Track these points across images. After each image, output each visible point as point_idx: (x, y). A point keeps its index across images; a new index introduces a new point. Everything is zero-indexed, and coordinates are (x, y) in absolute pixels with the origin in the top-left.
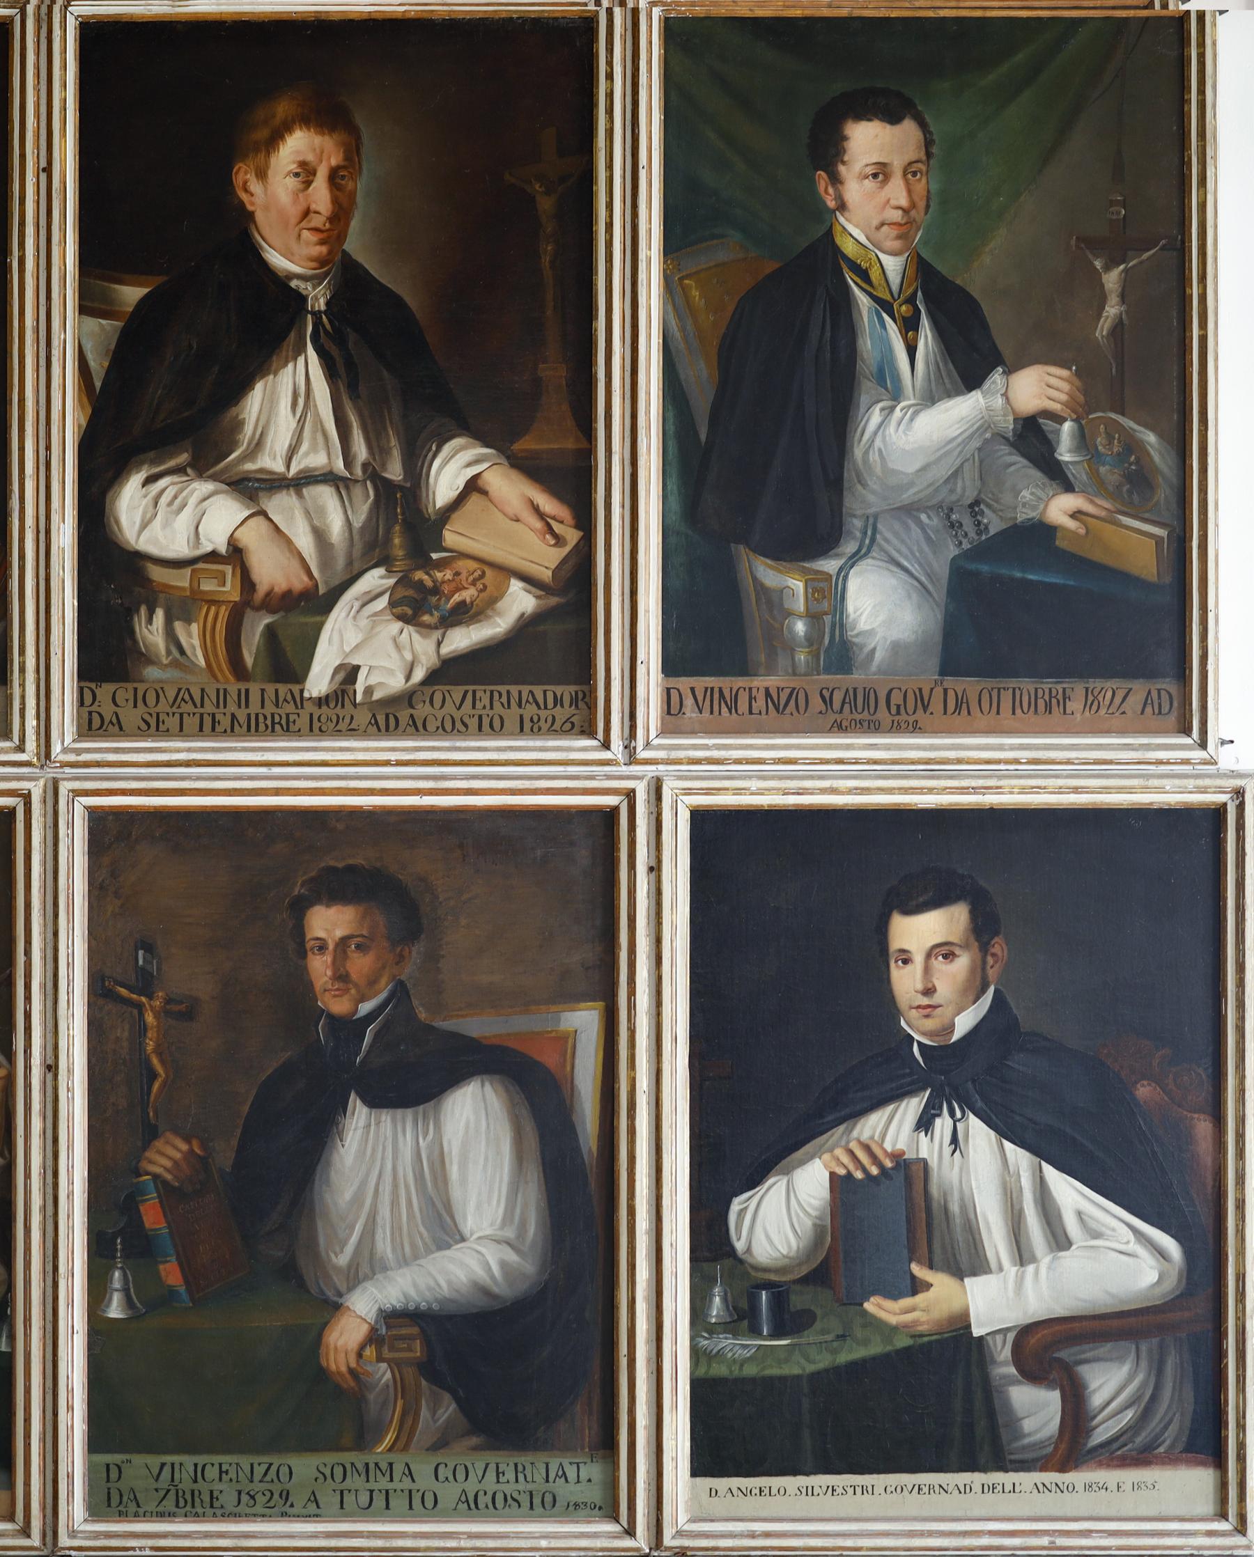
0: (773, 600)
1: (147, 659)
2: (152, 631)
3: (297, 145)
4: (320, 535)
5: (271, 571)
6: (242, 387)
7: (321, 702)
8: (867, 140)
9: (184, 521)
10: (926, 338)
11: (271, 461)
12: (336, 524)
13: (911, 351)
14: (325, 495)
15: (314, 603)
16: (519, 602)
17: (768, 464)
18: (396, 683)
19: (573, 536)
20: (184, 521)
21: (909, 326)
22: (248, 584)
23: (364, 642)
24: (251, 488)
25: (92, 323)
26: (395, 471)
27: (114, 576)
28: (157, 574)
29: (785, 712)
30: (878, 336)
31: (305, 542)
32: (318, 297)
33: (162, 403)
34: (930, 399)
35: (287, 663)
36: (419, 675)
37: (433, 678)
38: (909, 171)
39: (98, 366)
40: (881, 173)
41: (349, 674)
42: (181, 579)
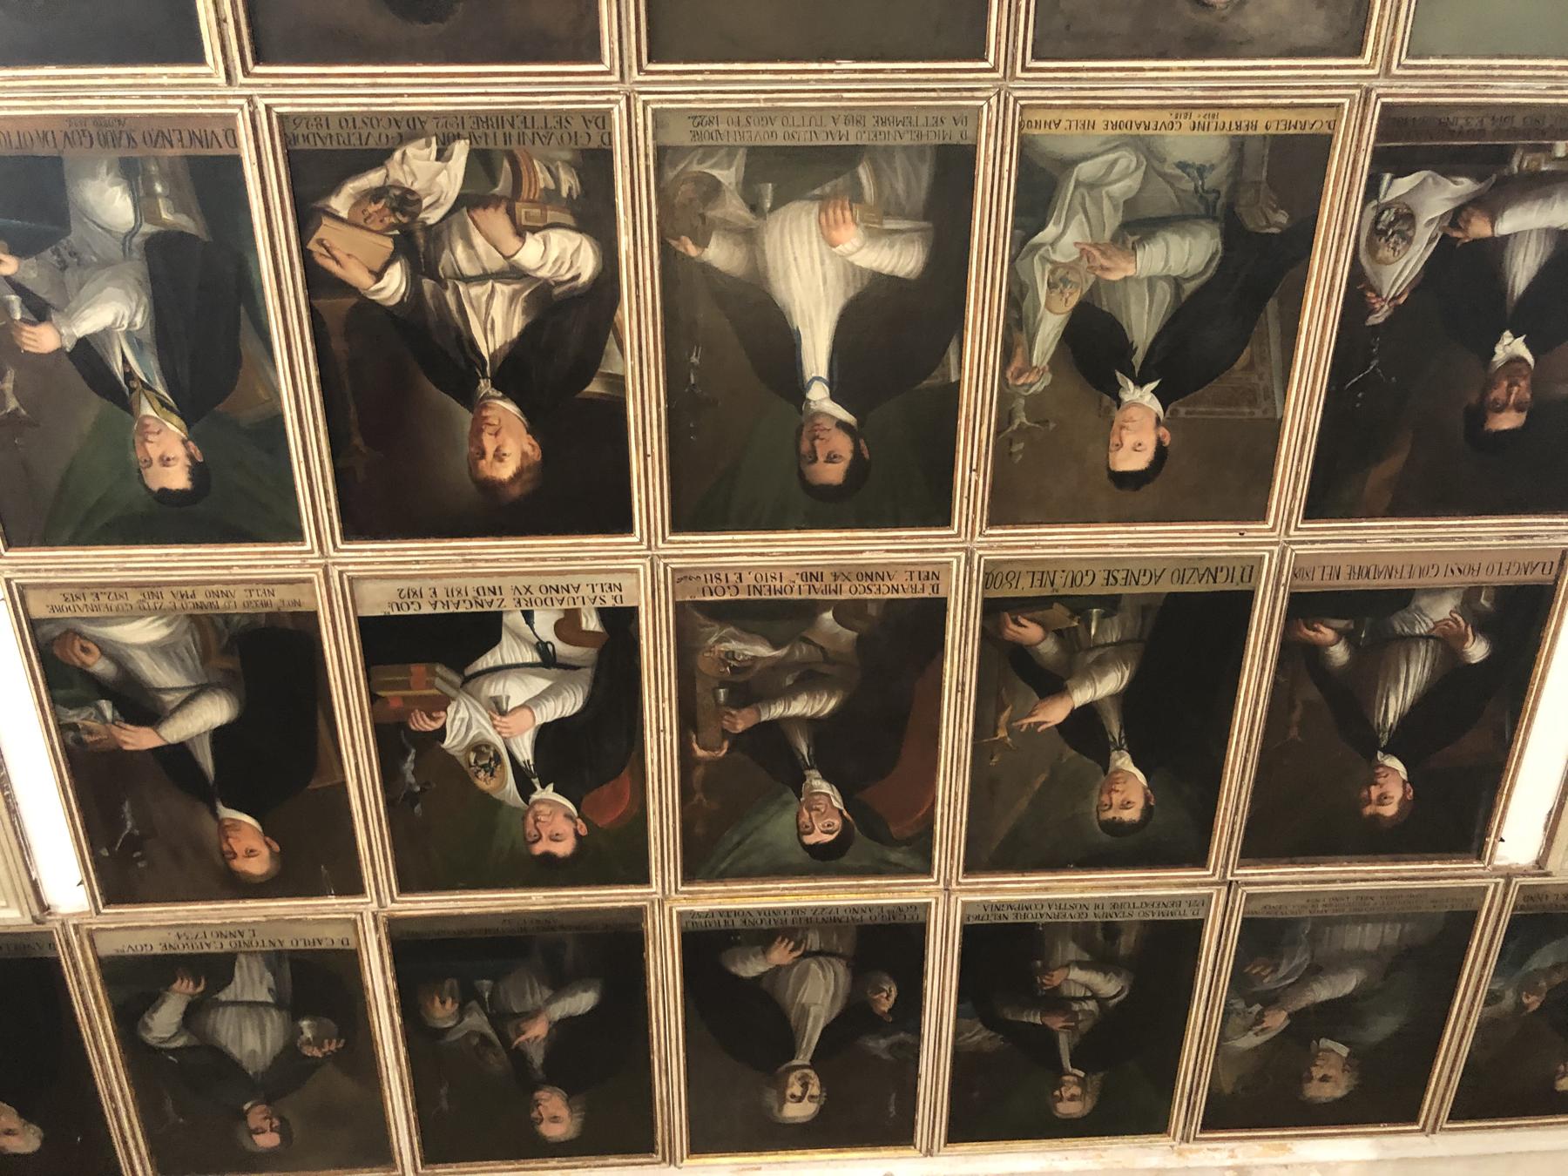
0: (179, 207)
1: (570, 164)
2: (568, 182)
3: (506, 471)
4: (469, 245)
5: (497, 221)
6: (524, 334)
7: (458, 137)
8: (177, 478)
9: (554, 253)
10: (118, 368)
11: (504, 291)
12: (460, 251)
13: (125, 360)
14: (468, 269)
15: (468, 201)
16: (340, 203)
18: (411, 150)
19: (312, 245)
20: (554, 253)
21: (129, 375)
22: (511, 213)
23: (434, 176)
24: (513, 273)
25: (617, 370)
26: (428, 284)
27: (593, 215)
28: (568, 219)
29: (159, 130)
30: (145, 368)
31: (478, 240)
32: (485, 386)
33: (569, 325)
34: (107, 332)
35: (481, 163)
36: (397, 155)
37: (389, 153)
38: (149, 463)
39: (611, 345)
40: (165, 461)
41: (442, 155)
42: (552, 216)
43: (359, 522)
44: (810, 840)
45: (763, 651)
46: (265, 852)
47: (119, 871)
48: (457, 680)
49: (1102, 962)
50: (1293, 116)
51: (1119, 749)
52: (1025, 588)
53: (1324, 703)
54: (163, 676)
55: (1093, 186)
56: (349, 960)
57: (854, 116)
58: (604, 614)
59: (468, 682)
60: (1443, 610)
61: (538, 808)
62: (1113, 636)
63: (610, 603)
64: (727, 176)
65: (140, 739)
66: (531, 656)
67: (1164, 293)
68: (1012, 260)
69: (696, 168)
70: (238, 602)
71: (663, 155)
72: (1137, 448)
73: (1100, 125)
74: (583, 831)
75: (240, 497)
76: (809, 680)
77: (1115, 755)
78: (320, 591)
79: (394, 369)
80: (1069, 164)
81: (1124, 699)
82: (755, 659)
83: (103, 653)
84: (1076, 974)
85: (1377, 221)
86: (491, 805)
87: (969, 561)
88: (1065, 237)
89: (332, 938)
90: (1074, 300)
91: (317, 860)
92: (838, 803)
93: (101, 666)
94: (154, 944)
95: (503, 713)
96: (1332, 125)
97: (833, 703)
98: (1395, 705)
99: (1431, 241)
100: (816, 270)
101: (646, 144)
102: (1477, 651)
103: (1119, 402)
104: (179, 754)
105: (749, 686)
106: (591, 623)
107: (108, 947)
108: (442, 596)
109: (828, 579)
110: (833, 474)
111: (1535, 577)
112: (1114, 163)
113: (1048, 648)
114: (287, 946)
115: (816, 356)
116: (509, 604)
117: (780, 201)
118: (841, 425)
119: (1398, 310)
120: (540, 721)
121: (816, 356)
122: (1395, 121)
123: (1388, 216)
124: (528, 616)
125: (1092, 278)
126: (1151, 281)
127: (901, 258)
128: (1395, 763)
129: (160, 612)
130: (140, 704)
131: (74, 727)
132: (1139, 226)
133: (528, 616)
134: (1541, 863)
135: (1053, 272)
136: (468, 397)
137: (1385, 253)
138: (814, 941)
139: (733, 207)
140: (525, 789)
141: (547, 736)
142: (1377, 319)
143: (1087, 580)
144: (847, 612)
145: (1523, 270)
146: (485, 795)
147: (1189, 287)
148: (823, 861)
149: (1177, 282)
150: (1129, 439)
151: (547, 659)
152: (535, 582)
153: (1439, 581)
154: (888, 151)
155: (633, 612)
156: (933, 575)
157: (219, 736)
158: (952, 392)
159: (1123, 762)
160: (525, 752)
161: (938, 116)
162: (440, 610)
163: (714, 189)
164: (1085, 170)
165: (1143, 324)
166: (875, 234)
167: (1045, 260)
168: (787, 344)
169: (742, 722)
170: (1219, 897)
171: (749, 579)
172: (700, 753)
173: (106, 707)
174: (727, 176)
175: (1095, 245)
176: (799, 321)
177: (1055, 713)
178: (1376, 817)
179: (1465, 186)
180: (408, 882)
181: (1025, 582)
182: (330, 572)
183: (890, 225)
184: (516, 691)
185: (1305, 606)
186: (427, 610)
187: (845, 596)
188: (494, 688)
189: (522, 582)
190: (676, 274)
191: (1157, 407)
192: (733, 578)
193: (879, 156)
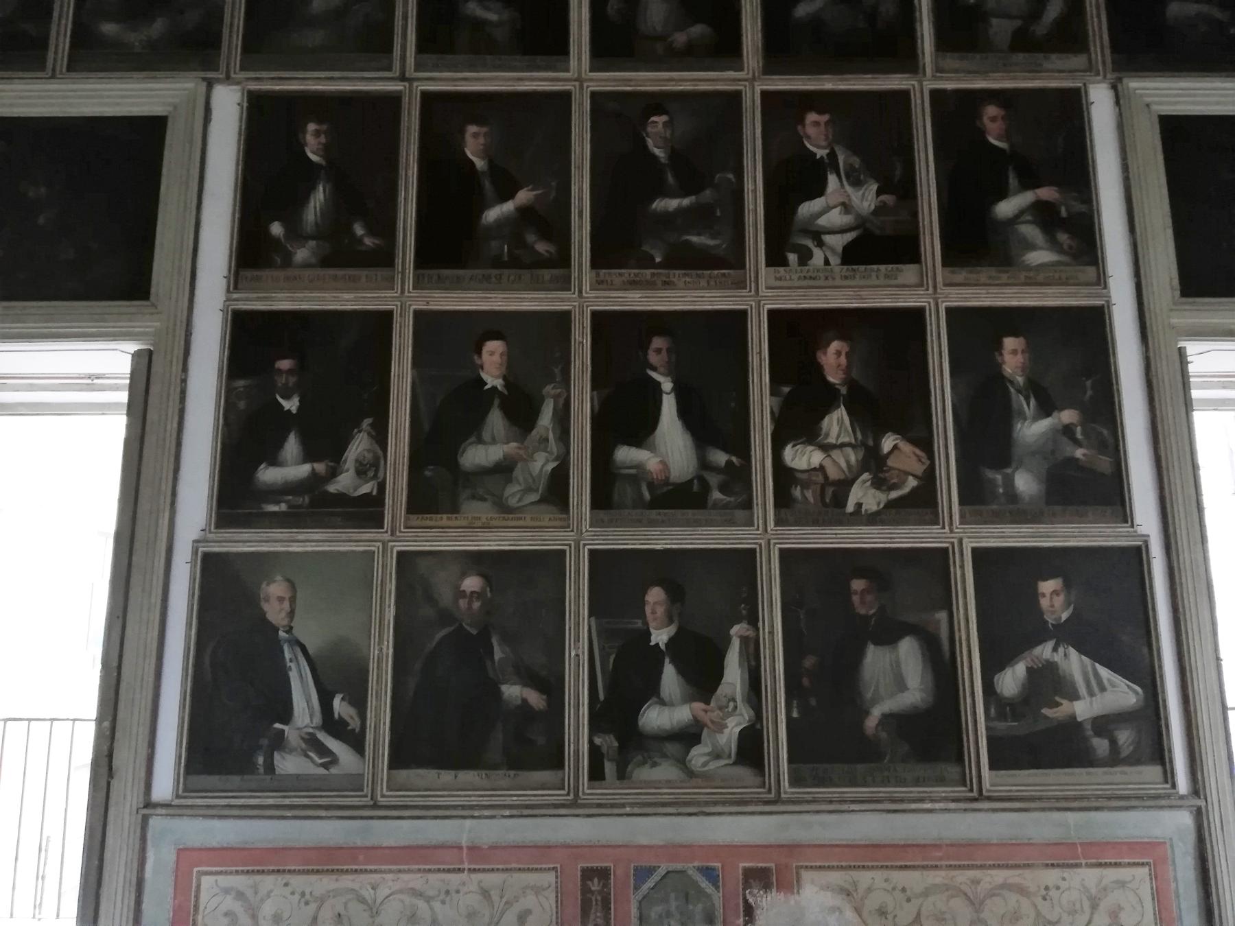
0: (992, 482)
1: (794, 500)
2: (797, 492)
3: (835, 345)
4: (848, 462)
5: (833, 474)
6: (823, 418)
7: (851, 514)
8: (1010, 343)
9: (805, 458)
10: (1033, 402)
11: (832, 440)
12: (853, 458)
13: (1028, 405)
14: (849, 450)
15: (845, 485)
16: (912, 483)
17: (986, 439)
18: (874, 508)
19: (928, 462)
20: (805, 458)
21: (1027, 399)
22: (826, 477)
23: (864, 495)
24: (826, 448)
25: (774, 399)
26: (871, 443)
27: (784, 477)
28: (799, 475)
29: (997, 518)
30: (1019, 400)
31: (844, 465)
32: (844, 390)
33: (797, 422)
34: (1036, 419)
35: (840, 500)
36: (882, 506)
37: (886, 506)
38: (1023, 352)
39: (776, 410)
40: (1014, 352)
41: (859, 505)
42: (804, 476)
43: (916, 317)
44: (664, 118)
45: (694, 239)
46: (986, 120)
47: (1071, 108)
48: (868, 225)
49: (479, 25)
50: (429, 523)
51: (483, 173)
52: (547, 274)
53: (363, 195)
54: (1030, 231)
55: (529, 490)
56: (944, 43)
57: (652, 523)
58: (784, 263)
59: (861, 224)
60: (301, 254)
61: (824, 143)
62: (494, 244)
63: (781, 269)
64: (716, 495)
65: (1047, 193)
66: (827, 238)
67: (486, 435)
68: (568, 452)
69: (732, 499)
70: (984, 274)
71: (748, 505)
72: (492, 354)
73: (528, 517)
74: (799, 128)
75: (977, 331)
76: (667, 218)
77: (486, 168)
78: (939, 279)
79: (890, 402)
80: (541, 501)
81: (484, 206)
82: (699, 234)
83: (1061, 245)
84: (493, 17)
85: (377, 472)
86: (854, 148)
87: (580, 292)
88: (542, 464)
89: (951, 61)
90: (534, 432)
91: (956, 112)
92: (650, 142)
93: (1063, 237)
94: (1056, 61)
95: (843, 204)
96: (407, 519)
97: (654, 206)
98: (319, 196)
99: (346, 461)
100: (671, 448)
101: (758, 511)
102: (276, 229)
103: (505, 378)
104: (1029, 183)
105: (700, 217)
106: (792, 257)
107: (1078, 61)
108: (874, 274)
109: (659, 283)
110: (658, 342)
111: (249, 273)
112: (520, 500)
113: (531, 238)
114: (978, 56)
115: (669, 405)
116: (837, 269)
117: (690, 482)
118: (654, 369)
119: (357, 424)
120: (823, 199)
121: (669, 405)
122: (376, 521)
123: (371, 474)
124: (827, 262)
125: (526, 443)
126: (494, 441)
127: (626, 454)
128: (314, 158)
129: (1028, 268)
130: (1044, 215)
131: (1083, 202)
132: (504, 469)
133: (827, 262)
134: (210, 84)
135: (546, 447)
136: (851, 383)
137: (369, 456)
138: (660, 48)
139: (714, 480)
140: (832, 155)
141: (818, 190)
142: (367, 422)
143: (512, 278)
144: (647, 262)
145: (292, 446)
146: (855, 153)
147: (473, 439)
148: (656, 103)
149: (480, 441)
150: (496, 358)
151: (817, 236)
152: (821, 283)
153: (308, 273)
154: (634, 507)
155: (769, 263)
156: (599, 284)
157: (1003, 194)
158: (596, 384)
159: (480, 164)
160: (832, 180)
161: (611, 523)
162: (875, 267)
163: (723, 488)
164: (534, 497)
165: (496, 420)
166: (639, 466)
167: (551, 453)
168: (684, 413)
169: (708, 195)
170: (410, 72)
171: (703, 283)
172: (731, 176)
173: (1064, 213)
174: (716, 495)
175: (525, 460)
176: (678, 424)
177: (524, 196)
178: (319, 121)
179: (332, 488)
180: (903, 97)
181: (547, 277)
182: (932, 291)
183: (633, 471)
184: (835, 218)
185: (384, 258)
186: (883, 267)
187: (648, 272)
188: (847, 220)
189: (830, 283)
190: (741, 446)
191: (484, 376)
192: (712, 283)
193: (639, 503)
